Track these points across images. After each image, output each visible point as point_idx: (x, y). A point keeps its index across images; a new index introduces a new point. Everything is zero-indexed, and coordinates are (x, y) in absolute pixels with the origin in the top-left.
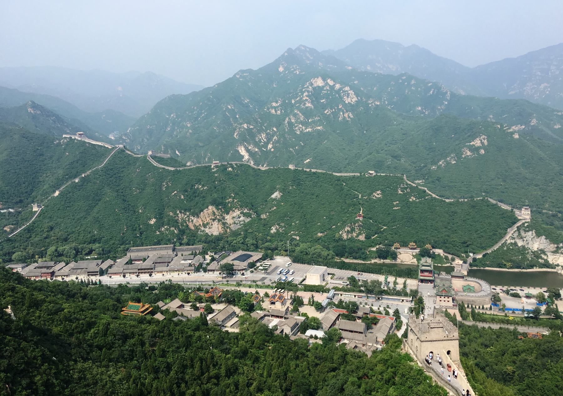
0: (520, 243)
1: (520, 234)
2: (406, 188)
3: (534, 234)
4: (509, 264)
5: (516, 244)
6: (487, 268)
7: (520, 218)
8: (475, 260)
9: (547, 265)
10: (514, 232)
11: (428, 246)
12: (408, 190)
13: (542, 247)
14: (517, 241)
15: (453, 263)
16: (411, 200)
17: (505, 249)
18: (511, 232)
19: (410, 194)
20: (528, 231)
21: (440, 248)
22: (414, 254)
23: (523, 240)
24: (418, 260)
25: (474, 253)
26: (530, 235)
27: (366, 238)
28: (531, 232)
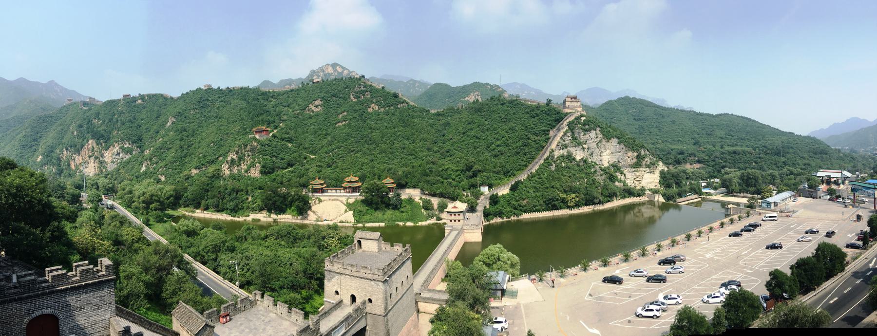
0: (579, 155)
2: (363, 93)
3: (601, 136)
4: (571, 197)
5: (570, 157)
6: (525, 216)
8: (494, 200)
10: (565, 134)
11: (388, 181)
14: (572, 150)
16: (370, 110)
17: (553, 168)
19: (369, 102)
21: (414, 187)
22: (351, 201)
23: (583, 148)
25: (490, 186)
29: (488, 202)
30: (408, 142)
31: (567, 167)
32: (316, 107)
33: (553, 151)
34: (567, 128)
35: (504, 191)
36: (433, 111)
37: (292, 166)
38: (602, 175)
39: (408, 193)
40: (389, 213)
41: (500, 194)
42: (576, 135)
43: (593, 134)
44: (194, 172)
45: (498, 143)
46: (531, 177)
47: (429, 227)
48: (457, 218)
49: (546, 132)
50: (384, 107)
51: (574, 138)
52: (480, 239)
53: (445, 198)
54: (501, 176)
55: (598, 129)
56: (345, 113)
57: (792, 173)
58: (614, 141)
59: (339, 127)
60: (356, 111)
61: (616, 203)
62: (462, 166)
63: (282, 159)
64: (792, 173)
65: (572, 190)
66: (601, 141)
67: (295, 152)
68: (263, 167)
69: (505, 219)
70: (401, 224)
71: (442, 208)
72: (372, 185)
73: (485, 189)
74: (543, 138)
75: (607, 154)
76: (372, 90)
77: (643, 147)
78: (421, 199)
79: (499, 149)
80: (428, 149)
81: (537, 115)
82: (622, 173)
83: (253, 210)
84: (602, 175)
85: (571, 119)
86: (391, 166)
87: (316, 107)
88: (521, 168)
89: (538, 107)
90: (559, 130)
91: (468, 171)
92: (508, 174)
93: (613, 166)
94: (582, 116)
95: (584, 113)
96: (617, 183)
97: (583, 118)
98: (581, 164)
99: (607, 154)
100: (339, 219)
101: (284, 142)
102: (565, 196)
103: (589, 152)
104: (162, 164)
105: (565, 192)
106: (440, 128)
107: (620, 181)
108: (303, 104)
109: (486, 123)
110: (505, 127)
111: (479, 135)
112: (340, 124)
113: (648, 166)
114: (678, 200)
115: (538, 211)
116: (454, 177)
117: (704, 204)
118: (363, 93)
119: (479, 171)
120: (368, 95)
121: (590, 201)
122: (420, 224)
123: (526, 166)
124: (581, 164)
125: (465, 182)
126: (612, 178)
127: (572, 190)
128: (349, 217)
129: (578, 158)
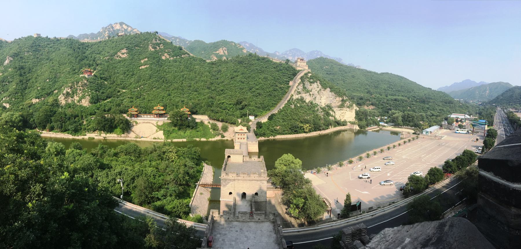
0: (308, 99)
1: (304, 88)
2: (159, 45)
3: (320, 87)
4: (306, 126)
5: (302, 100)
6: (279, 137)
7: (298, 69)
8: (259, 125)
9: (338, 123)
10: (299, 84)
11: (185, 110)
12: (162, 47)
13: (328, 102)
14: (304, 95)
15: (225, 134)
16: (163, 58)
17: (293, 107)
18: (295, 85)
19: (163, 51)
20: (313, 83)
21: (202, 114)
23: (310, 95)
24: (168, 134)
25: (256, 116)
26: (315, 87)
27: (91, 103)
28: (315, 83)
29: (256, 126)
30: (193, 82)
31: (301, 107)
32: (123, 54)
33: (292, 95)
34: (300, 80)
35: (264, 120)
36: (208, 61)
37: (110, 98)
38: (322, 112)
39: (198, 118)
40: (188, 132)
41: (262, 122)
42: (306, 86)
43: (315, 85)
44: (34, 101)
45: (257, 87)
46: (280, 112)
47: (216, 142)
48: (243, 136)
49: (287, 83)
50: (173, 56)
51: (304, 88)
52: (258, 151)
53: (226, 122)
54: (261, 110)
55: (318, 82)
56: (146, 59)
57: (433, 115)
58: (328, 89)
59: (142, 69)
60: (154, 58)
61: (332, 130)
62: (234, 101)
63: (103, 93)
64: (433, 115)
65: (306, 122)
66: (320, 90)
67: (110, 88)
68: (92, 98)
69: (266, 138)
70: (198, 139)
71: (225, 129)
72: (176, 112)
73: (252, 118)
74: (286, 86)
75: (324, 98)
76: (165, 43)
77: (345, 94)
78: (209, 122)
79: (258, 91)
80: (209, 88)
81: (281, 70)
82: (333, 111)
83: (89, 130)
84: (322, 112)
85: (302, 74)
86: (183, 99)
87: (123, 54)
88: (274, 105)
89: (281, 64)
90: (295, 82)
91: (239, 104)
92: (266, 108)
93: (328, 106)
94: (309, 73)
95: (310, 71)
96: (330, 118)
97: (310, 75)
98: (310, 105)
99: (324, 98)
100: (153, 137)
101: (102, 81)
102: (302, 125)
103: (314, 97)
104: (5, 95)
105: (301, 122)
106: (214, 74)
107: (332, 116)
108: (112, 52)
109: (247, 72)
110: (260, 76)
111: (243, 80)
112: (143, 67)
113: (348, 107)
114: (367, 129)
115: (286, 134)
116: (229, 108)
117: (381, 131)
118: (159, 45)
119: (246, 105)
120: (162, 47)
121: (317, 128)
122: (210, 139)
123: (276, 104)
124: (310, 105)
125: (238, 113)
126: (328, 114)
127: (306, 122)
128: (161, 136)
129: (307, 101)
